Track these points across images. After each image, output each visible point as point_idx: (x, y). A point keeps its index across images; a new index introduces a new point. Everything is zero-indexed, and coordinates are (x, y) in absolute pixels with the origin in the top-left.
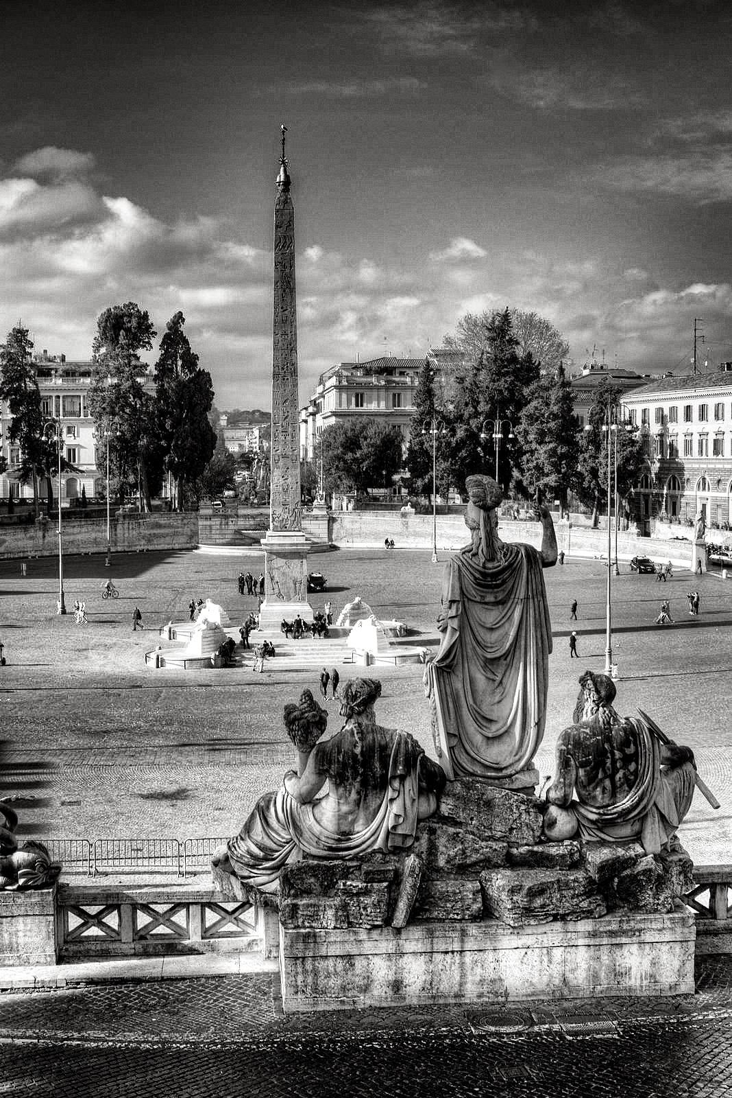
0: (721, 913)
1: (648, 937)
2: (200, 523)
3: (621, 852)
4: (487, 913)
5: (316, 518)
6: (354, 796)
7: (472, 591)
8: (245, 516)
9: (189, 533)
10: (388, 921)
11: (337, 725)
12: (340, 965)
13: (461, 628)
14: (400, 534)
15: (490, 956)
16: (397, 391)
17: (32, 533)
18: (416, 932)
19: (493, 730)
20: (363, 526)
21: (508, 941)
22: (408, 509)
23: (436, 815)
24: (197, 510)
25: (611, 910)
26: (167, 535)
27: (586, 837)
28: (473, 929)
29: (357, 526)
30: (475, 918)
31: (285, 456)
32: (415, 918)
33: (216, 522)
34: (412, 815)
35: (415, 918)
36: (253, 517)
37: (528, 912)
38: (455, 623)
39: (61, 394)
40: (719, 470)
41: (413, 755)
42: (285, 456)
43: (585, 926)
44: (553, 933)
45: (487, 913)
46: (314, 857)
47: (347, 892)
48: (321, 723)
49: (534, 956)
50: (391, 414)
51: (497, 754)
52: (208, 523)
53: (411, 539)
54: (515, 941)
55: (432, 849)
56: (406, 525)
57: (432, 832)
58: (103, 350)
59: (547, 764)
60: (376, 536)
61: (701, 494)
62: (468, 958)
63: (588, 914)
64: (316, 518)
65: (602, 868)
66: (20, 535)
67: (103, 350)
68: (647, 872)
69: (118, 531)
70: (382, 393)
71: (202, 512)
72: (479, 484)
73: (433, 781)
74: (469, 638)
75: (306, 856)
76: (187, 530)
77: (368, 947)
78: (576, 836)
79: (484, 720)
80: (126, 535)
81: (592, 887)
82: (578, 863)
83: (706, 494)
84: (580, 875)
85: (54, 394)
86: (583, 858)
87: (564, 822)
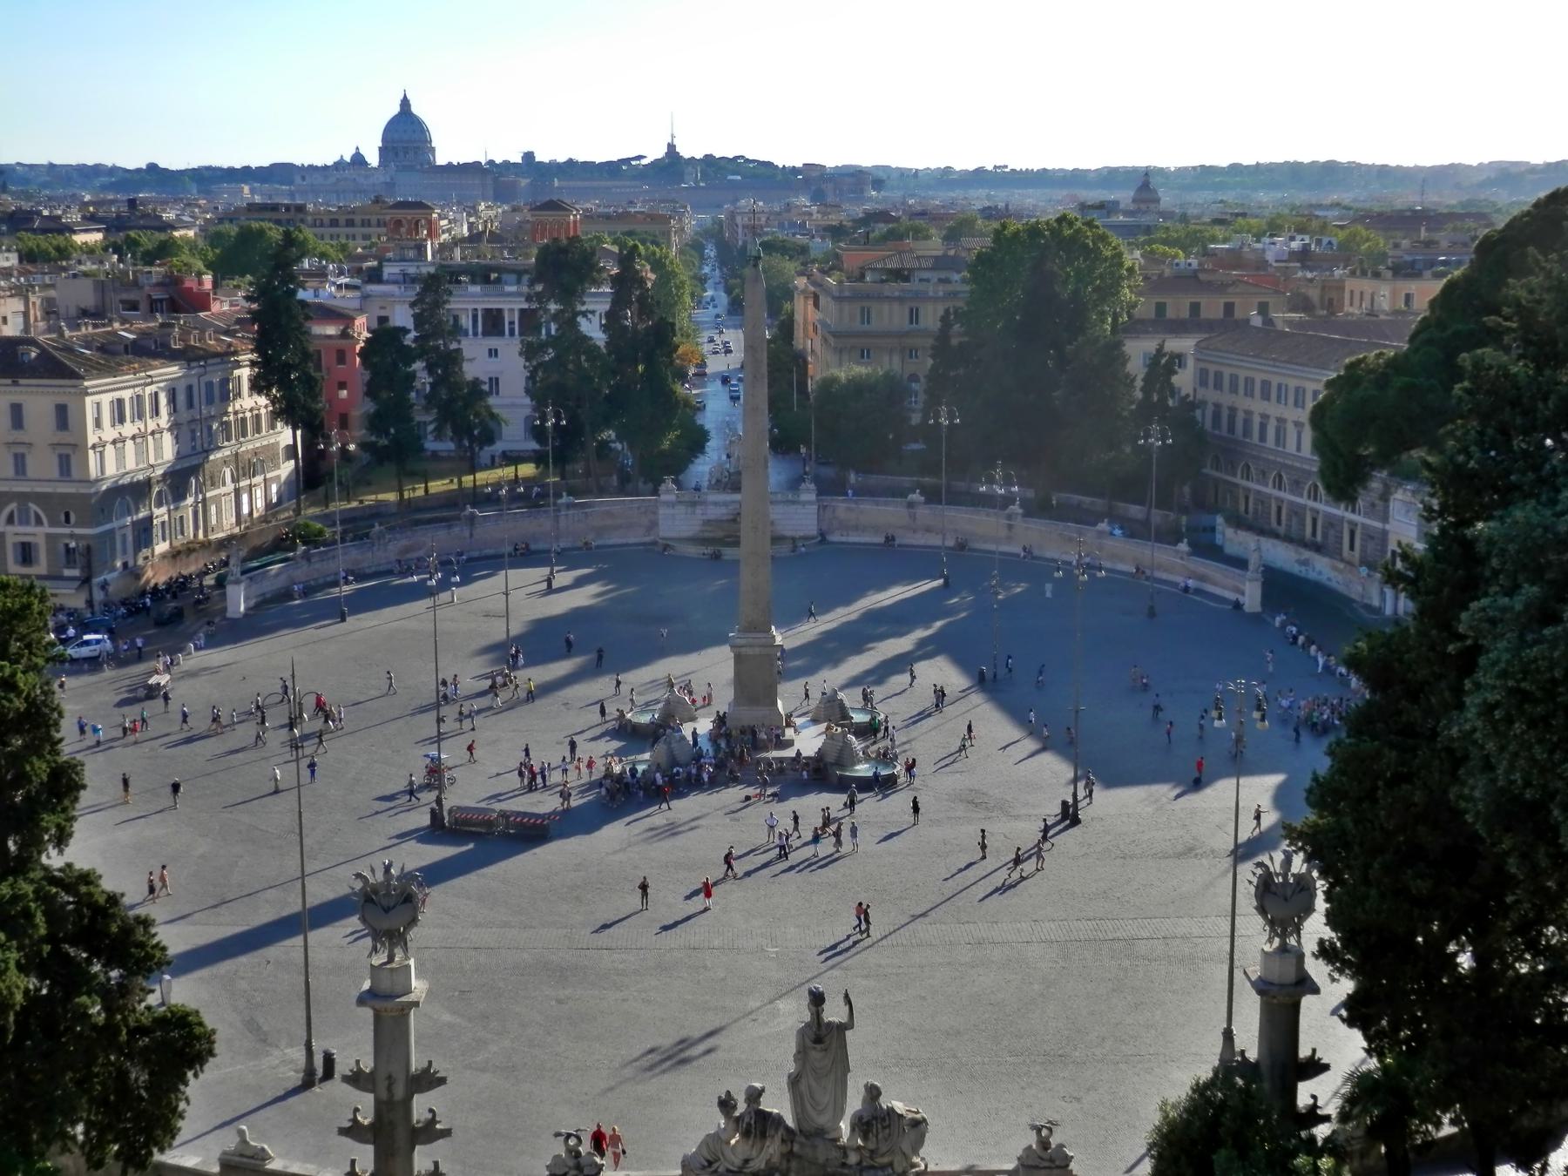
2: (662, 511)
5: (804, 503)
7: (809, 1043)
8: (716, 504)
11: (742, 1107)
16: (914, 305)
17: (456, 530)
22: (916, 497)
33: (680, 509)
36: (725, 504)
40: (1297, 469)
41: (778, 1121)
48: (734, 1107)
50: (907, 334)
51: (822, 1120)
52: (670, 511)
56: (913, 517)
59: (844, 1126)
64: (804, 503)
70: (896, 306)
71: (664, 497)
78: (859, 1163)
83: (1282, 494)
87: (853, 1159)
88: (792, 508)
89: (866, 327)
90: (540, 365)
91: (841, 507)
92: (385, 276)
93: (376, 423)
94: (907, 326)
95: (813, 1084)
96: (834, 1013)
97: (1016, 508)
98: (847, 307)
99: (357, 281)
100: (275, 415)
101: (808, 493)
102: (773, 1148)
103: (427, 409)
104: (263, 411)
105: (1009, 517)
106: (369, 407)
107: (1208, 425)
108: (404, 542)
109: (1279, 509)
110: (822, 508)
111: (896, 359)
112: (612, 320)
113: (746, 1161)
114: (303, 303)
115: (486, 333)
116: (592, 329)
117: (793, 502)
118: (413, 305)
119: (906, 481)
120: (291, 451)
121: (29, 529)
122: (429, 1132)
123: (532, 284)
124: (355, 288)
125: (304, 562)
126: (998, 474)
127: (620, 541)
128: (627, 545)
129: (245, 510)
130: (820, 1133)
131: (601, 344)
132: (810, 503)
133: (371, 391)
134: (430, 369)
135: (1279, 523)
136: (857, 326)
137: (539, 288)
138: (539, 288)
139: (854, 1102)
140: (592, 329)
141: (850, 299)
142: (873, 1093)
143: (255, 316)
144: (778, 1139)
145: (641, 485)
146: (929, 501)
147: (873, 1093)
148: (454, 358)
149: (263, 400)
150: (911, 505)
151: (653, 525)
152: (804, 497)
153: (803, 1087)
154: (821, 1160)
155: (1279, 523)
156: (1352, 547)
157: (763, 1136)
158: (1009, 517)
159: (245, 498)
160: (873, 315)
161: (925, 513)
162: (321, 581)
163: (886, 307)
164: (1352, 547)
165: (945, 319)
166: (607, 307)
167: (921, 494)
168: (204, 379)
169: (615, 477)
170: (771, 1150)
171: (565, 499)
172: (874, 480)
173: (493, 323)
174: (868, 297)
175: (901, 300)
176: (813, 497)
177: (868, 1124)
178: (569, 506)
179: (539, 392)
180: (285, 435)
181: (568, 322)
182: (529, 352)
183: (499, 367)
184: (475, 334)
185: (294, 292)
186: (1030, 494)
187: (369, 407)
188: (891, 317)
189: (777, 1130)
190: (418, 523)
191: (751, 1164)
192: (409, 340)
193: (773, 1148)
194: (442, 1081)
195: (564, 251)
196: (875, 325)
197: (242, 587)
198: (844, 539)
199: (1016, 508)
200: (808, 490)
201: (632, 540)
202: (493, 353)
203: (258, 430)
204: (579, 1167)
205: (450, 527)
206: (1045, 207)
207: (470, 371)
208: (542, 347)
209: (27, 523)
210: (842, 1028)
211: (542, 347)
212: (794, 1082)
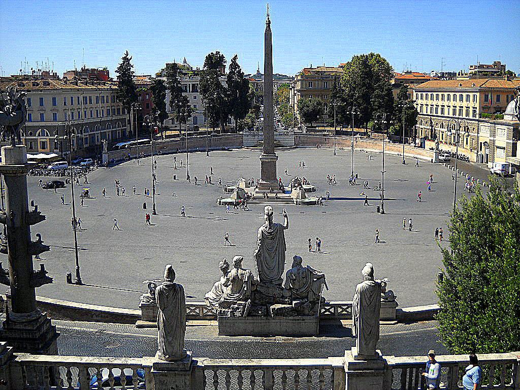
0: (336, 314)
18: (250, 318)
35: (249, 314)
51: (273, 275)
57: (255, 294)
58: (205, 68)
61: (441, 129)
65: (295, 304)
67: (205, 68)
72: (268, 210)
78: (291, 296)
107: (419, 111)
109: (443, 134)
115: (192, 92)
121: (44, 137)
122: (39, 248)
135: (442, 139)
139: (288, 266)
142: (297, 261)
147: (297, 261)
155: (442, 139)
156: (467, 144)
164: (467, 144)
168: (102, 95)
173: (194, 89)
188: (319, 85)
194: (43, 218)
202: (195, 98)
203: (119, 113)
209: (44, 136)
212: (258, 256)
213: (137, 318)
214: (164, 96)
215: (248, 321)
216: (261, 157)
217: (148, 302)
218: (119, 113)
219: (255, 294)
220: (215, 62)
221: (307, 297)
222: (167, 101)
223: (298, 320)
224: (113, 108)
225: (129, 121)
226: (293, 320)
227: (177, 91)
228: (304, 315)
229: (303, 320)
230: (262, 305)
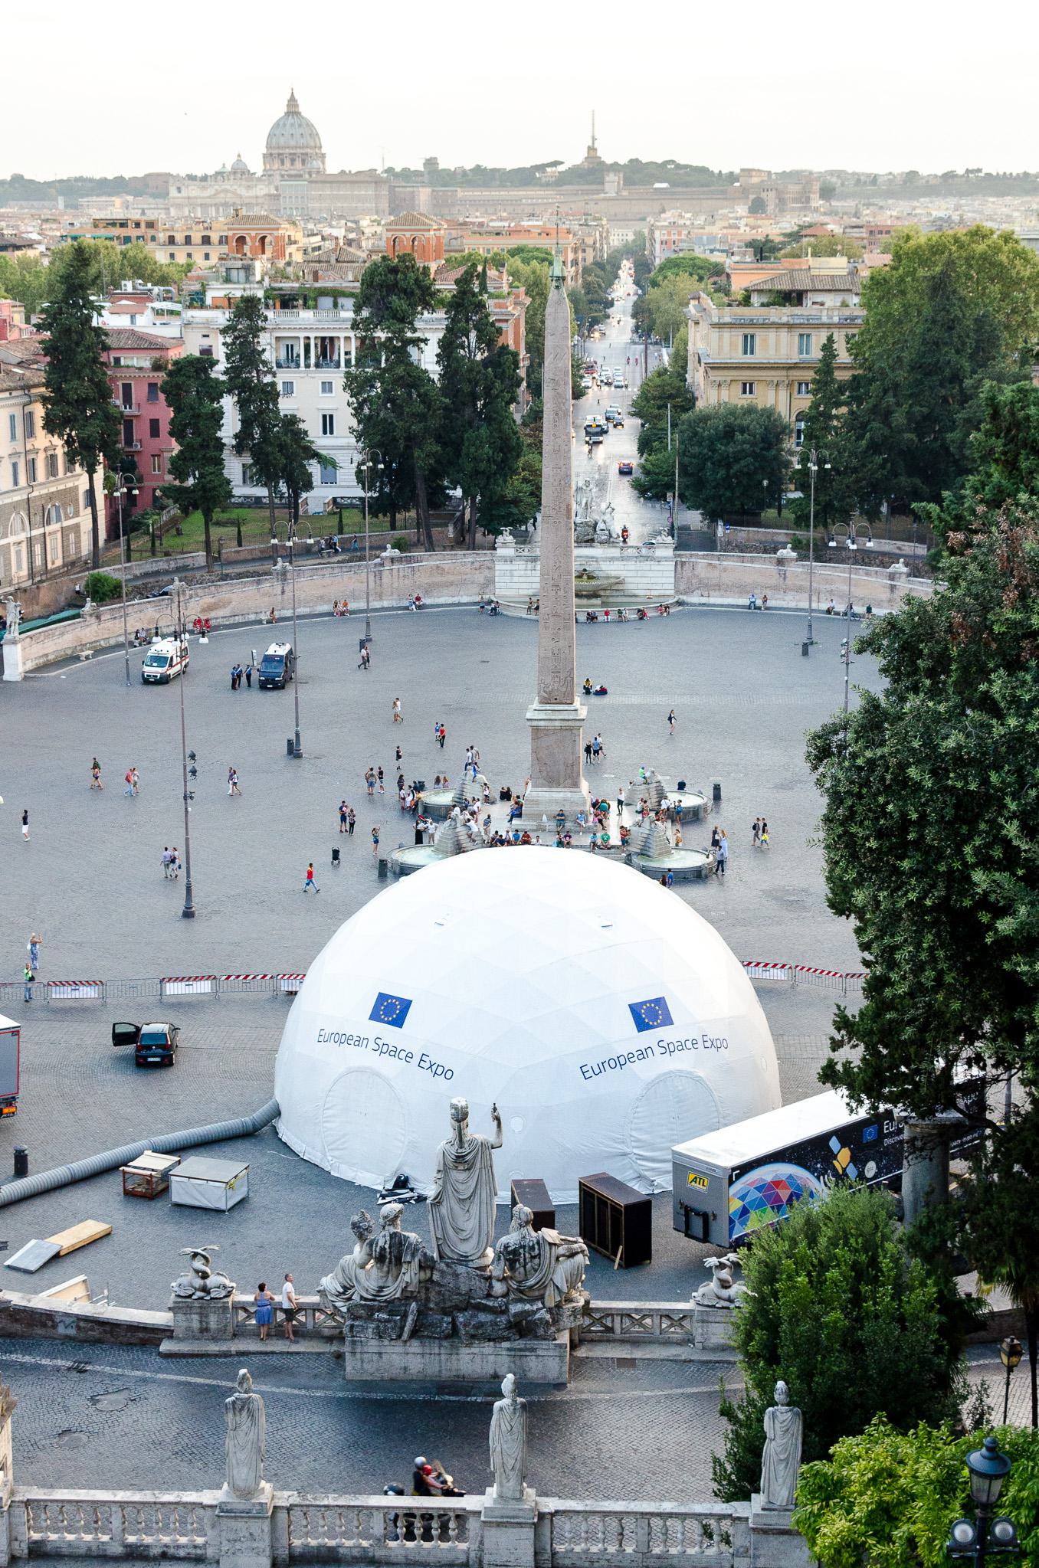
1: (540, 1353)
2: (497, 567)
3: (528, 1307)
4: (454, 1333)
6: (385, 1269)
9: (482, 580)
10: (400, 1336)
12: (375, 1357)
13: (445, 1183)
14: (776, 588)
15: (454, 1357)
18: (415, 1343)
19: (463, 1235)
20: (724, 575)
21: (464, 1351)
22: (787, 553)
23: (430, 1280)
24: (495, 549)
25: (522, 1336)
26: (452, 584)
27: (512, 1296)
28: (445, 1343)
29: (716, 573)
30: (447, 1337)
31: (556, 615)
32: (414, 1334)
33: (519, 566)
34: (415, 1281)
35: (414, 1334)
37: (473, 1337)
38: (440, 1182)
39: (312, 335)
42: (556, 615)
43: (506, 1345)
44: (488, 1348)
45: (454, 1333)
46: (366, 1299)
47: (379, 1320)
49: (478, 1359)
51: (465, 1248)
52: (508, 567)
53: (789, 596)
54: (467, 1350)
55: (428, 1299)
57: (427, 1289)
60: (742, 589)
62: (443, 1357)
63: (508, 1339)
65: (515, 1315)
66: (251, 589)
68: (540, 1319)
69: (385, 580)
70: (784, 334)
71: (500, 552)
73: (427, 1264)
74: (449, 1187)
75: (362, 1298)
76: (480, 577)
77: (389, 1349)
79: (458, 1230)
80: (395, 585)
81: (510, 1326)
82: (505, 1312)
84: (503, 1319)
85: (302, 335)
86: (507, 1308)
87: (499, 1288)
88: (646, 566)
89: (749, 359)
90: (365, 400)
91: (701, 562)
92: (209, 301)
93: (179, 468)
94: (795, 359)
95: (456, 1207)
96: (479, 1130)
97: (900, 567)
98: (727, 334)
99: (178, 307)
100: (71, 459)
101: (666, 548)
102: (410, 1274)
103: (239, 449)
104: (60, 452)
105: (892, 577)
106: (176, 448)
108: (208, 600)
110: (680, 565)
111: (783, 394)
112: (448, 347)
113: (381, 1289)
114: (99, 331)
116: (428, 359)
117: (647, 558)
118: (224, 331)
119: (781, 535)
120: (91, 493)
123: (358, 309)
124: (178, 314)
125: (93, 619)
126: (853, 529)
127: (450, 600)
128: (460, 604)
129: (38, 562)
130: (464, 1260)
131: (436, 377)
132: (666, 559)
133: (177, 432)
134: (242, 404)
136: (739, 357)
137: (365, 313)
138: (365, 313)
140: (428, 359)
141: (731, 326)
143: (50, 349)
144: (415, 1264)
145: (479, 536)
146: (802, 558)
148: (270, 394)
149: (57, 441)
150: (781, 562)
151: (490, 581)
152: (659, 553)
153: (444, 1210)
154: (464, 1289)
157: (399, 1262)
158: (892, 577)
159: (38, 549)
160: (757, 340)
161: (797, 570)
162: (112, 642)
163: (772, 335)
165: (828, 348)
166: (441, 335)
167: (793, 549)
169: (451, 528)
170: (407, 1278)
171: (390, 552)
172: (744, 533)
174: (752, 324)
175: (790, 327)
176: (670, 552)
177: (515, 1252)
178: (392, 560)
179: (375, 432)
180: (80, 480)
181: (399, 351)
182: (356, 385)
183: (319, 402)
184: (307, 366)
185: (89, 318)
186: (922, 550)
187: (176, 448)
188: (778, 347)
189: (413, 1256)
190: (225, 577)
191: (386, 1291)
192: (218, 372)
193: (410, 1274)
195: (394, 270)
196: (760, 356)
197: (19, 646)
198: (704, 600)
199: (900, 567)
200: (664, 545)
201: (465, 599)
202: (327, 387)
204: (205, 1290)
205: (258, 582)
206: (924, 218)
207: (286, 406)
208: (369, 382)
210: (487, 1148)
211: (369, 382)
213: (167, 1333)
214: (217, 416)
215: (412, 1350)
216: (529, 715)
217: (190, 1296)
218: (52, 469)
219: (427, 1289)
220: (392, 289)
221: (542, 1298)
222: (230, 425)
223: (521, 1350)
224: (30, 457)
225: (91, 493)
226: (509, 1349)
227: (258, 400)
228: (536, 1337)
229: (533, 1350)
230: (445, 1312)
